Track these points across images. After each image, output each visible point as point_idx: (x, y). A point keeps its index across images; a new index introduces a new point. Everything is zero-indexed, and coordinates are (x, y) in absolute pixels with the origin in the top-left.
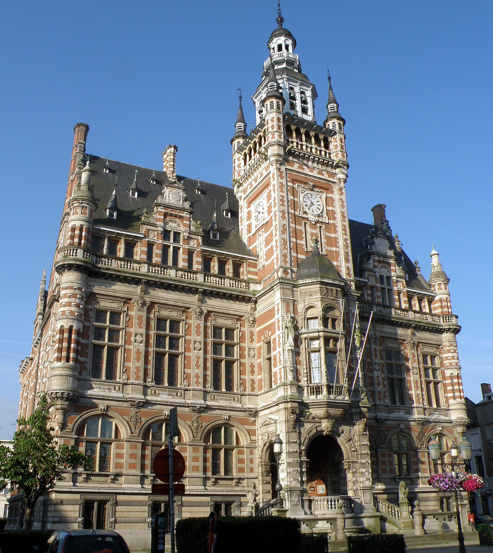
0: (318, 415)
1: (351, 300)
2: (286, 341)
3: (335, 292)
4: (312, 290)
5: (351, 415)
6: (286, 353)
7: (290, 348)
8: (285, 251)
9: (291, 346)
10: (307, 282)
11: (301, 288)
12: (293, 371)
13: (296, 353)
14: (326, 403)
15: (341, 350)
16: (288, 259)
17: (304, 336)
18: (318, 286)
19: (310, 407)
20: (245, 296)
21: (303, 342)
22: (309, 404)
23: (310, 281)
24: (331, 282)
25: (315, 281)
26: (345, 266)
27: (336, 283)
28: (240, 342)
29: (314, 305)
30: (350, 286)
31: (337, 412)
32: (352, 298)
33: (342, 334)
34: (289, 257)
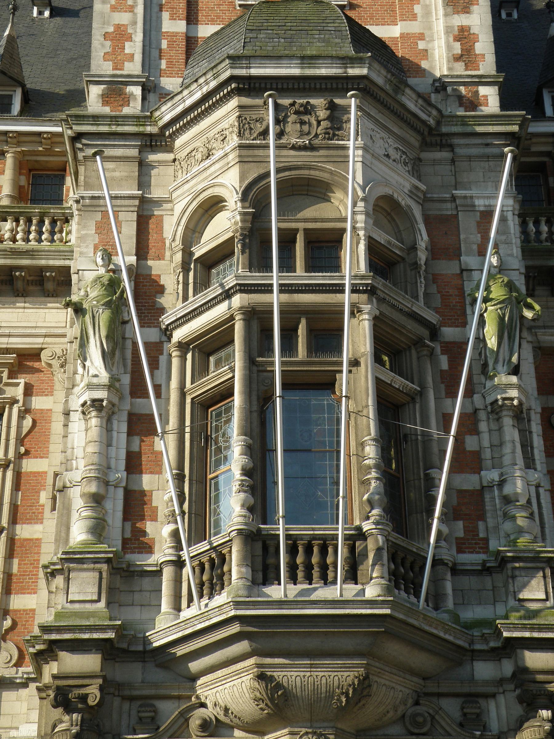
0: (233, 707)
1: (470, 158)
2: (80, 370)
3: (322, 114)
4: (211, 134)
5: (474, 698)
6: (77, 423)
7: (87, 397)
8: (123, 18)
9: (90, 387)
10: (189, 102)
11: (179, 142)
12: (96, 500)
13: (126, 415)
14: (235, 628)
15: (355, 363)
16: (135, 47)
17: (179, 335)
18: (234, 102)
19: (195, 666)
20: (41, 270)
21: (175, 362)
22: (181, 651)
23: (198, 96)
24: (295, 71)
25: (213, 84)
26: (448, 30)
27: (323, 72)
28: (20, 457)
29: (217, 191)
30: (473, 104)
31: (336, 676)
32: (474, 151)
33: (355, 290)
34: (139, 37)
